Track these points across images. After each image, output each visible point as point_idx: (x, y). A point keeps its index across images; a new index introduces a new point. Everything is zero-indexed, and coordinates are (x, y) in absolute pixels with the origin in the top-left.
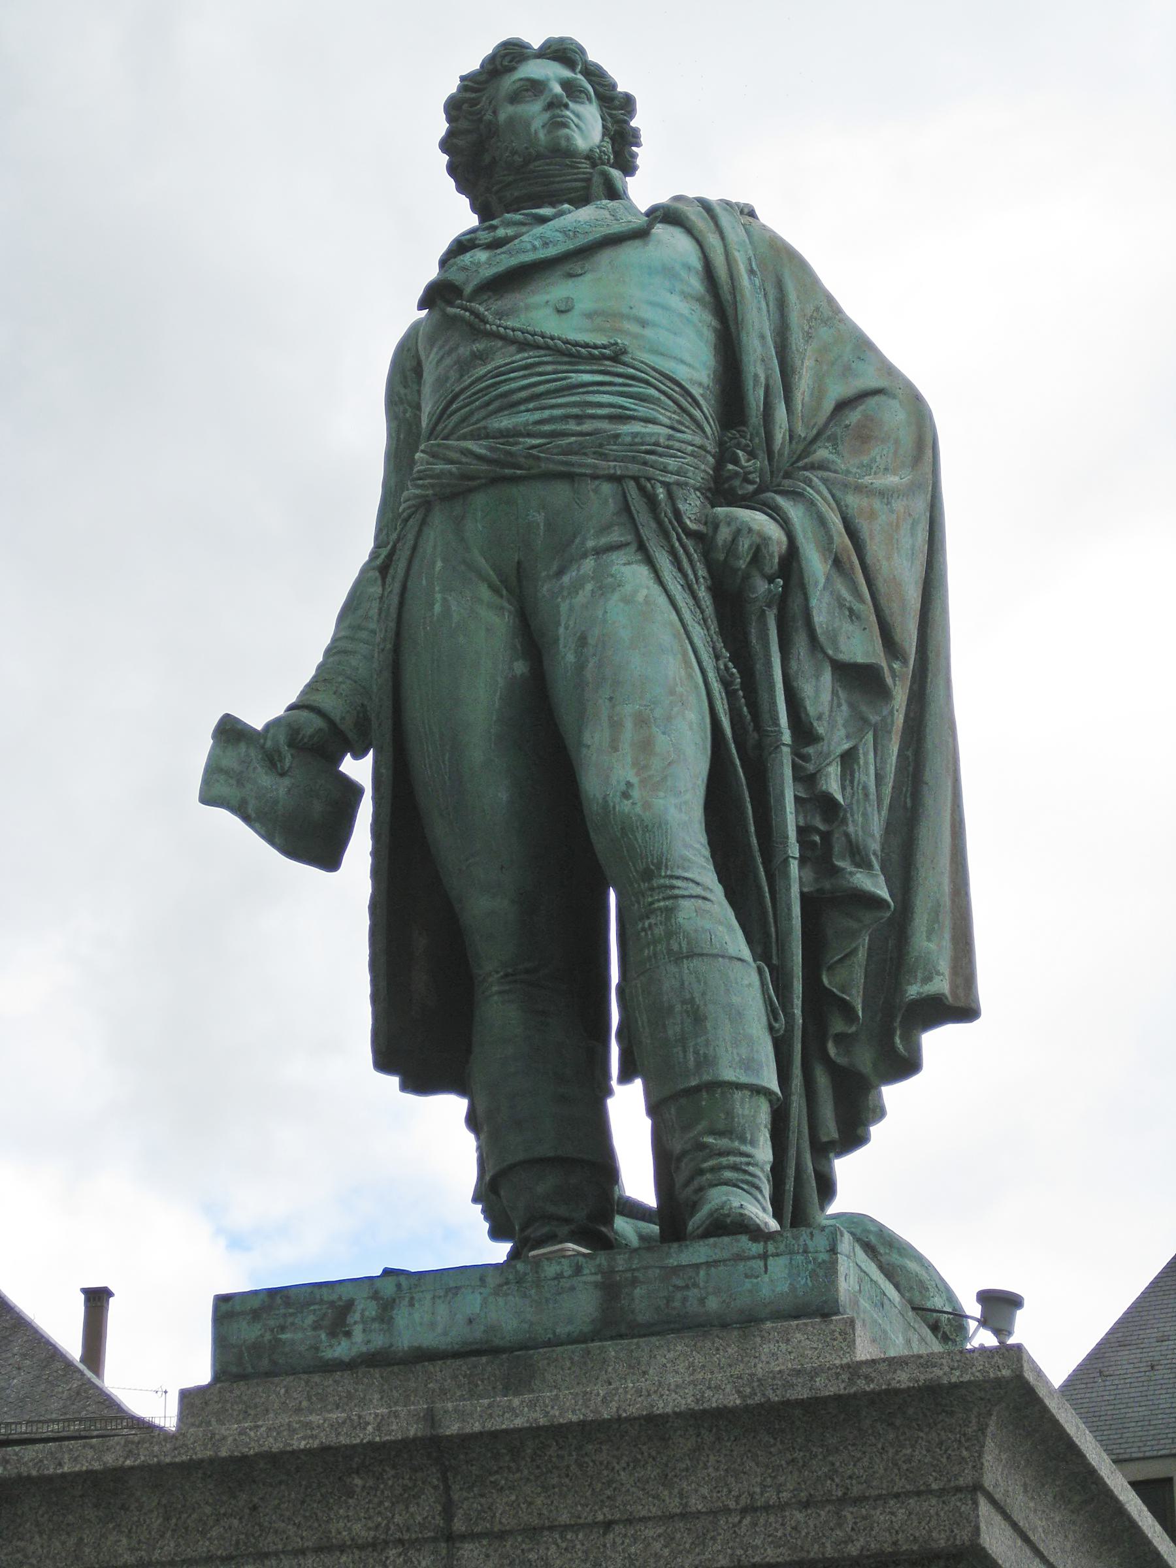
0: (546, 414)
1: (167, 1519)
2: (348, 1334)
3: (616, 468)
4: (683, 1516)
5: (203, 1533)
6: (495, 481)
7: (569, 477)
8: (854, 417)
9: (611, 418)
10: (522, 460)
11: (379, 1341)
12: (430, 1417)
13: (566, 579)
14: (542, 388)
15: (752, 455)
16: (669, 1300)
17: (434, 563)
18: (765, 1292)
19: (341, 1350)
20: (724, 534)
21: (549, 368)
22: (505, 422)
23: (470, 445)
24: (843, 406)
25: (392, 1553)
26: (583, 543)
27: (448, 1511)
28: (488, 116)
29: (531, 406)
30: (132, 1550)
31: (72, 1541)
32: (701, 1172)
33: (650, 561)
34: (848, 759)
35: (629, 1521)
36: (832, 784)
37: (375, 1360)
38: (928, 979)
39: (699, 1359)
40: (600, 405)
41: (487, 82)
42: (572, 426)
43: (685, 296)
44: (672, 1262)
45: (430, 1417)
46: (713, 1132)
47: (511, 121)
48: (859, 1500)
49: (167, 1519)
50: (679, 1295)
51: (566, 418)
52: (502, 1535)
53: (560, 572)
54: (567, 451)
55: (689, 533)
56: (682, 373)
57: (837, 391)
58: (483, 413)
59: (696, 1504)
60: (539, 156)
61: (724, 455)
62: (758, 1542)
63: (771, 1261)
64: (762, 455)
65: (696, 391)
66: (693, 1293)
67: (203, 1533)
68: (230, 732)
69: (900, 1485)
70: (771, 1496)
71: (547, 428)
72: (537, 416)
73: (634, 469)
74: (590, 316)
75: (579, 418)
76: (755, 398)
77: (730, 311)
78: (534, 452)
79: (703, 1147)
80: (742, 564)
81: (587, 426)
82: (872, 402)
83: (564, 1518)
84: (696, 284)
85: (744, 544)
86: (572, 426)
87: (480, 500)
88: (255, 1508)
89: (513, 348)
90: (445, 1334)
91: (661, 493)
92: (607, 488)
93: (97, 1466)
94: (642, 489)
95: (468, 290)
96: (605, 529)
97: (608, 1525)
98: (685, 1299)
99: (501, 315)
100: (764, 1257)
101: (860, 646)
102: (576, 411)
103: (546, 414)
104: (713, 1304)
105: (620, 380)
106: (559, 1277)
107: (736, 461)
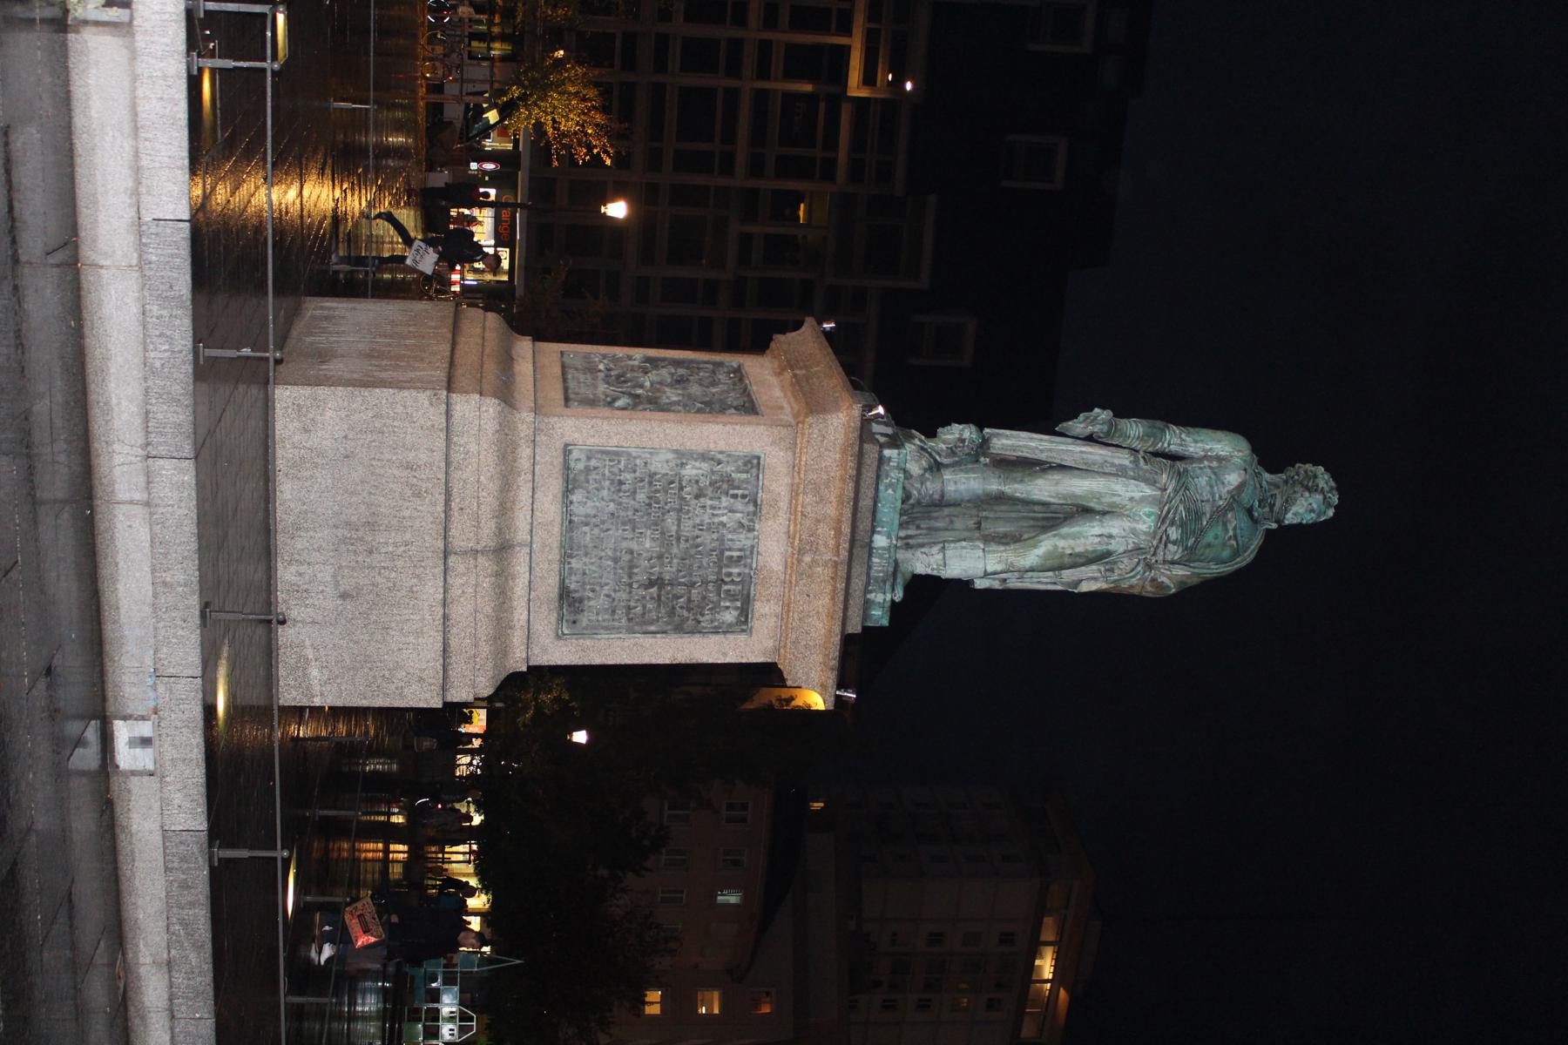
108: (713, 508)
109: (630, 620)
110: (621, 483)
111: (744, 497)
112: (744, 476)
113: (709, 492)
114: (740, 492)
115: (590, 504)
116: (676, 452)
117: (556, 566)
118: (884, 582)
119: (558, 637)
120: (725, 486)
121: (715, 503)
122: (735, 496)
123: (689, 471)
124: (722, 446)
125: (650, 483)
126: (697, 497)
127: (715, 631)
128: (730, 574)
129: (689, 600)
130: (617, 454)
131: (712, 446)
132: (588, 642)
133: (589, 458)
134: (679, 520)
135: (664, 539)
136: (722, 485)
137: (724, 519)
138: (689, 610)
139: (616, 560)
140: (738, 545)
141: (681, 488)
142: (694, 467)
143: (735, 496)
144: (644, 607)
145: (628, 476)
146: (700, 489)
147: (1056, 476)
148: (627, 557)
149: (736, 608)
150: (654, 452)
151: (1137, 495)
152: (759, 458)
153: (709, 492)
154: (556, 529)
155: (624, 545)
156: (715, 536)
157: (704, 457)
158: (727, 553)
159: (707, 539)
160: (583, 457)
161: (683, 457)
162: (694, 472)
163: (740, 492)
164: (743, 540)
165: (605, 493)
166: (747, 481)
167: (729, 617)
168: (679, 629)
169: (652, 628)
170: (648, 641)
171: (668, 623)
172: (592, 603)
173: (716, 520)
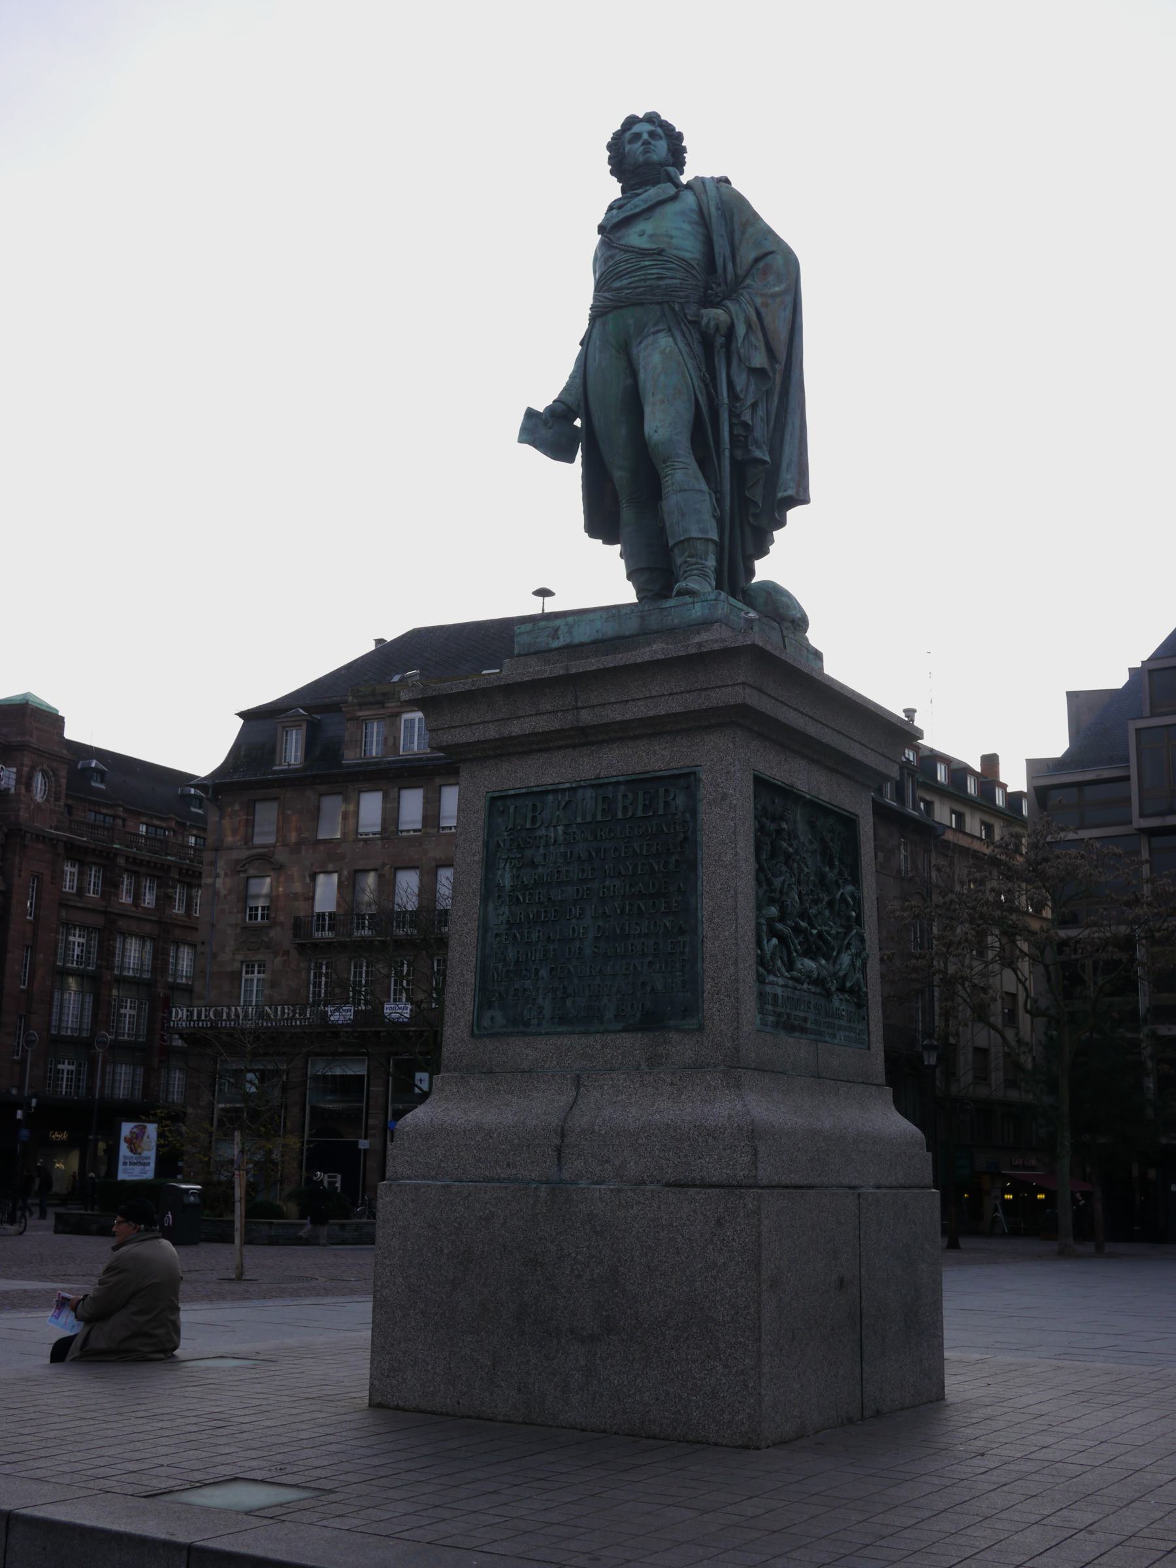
4: (650, 697)
7: (641, 304)
8: (761, 265)
9: (658, 279)
11: (568, 640)
12: (567, 668)
13: (642, 345)
15: (719, 285)
19: (555, 644)
20: (705, 321)
22: (617, 284)
24: (757, 260)
33: (673, 336)
34: (754, 406)
35: (633, 700)
36: (747, 417)
38: (785, 490)
42: (642, 284)
43: (690, 223)
45: (567, 668)
46: (690, 556)
48: (706, 689)
51: (640, 280)
52: (593, 707)
54: (641, 294)
55: (690, 322)
56: (687, 255)
57: (753, 255)
59: (654, 693)
61: (707, 287)
65: (693, 263)
66: (670, 618)
68: (530, 414)
70: (678, 689)
74: (651, 236)
75: (645, 280)
76: (719, 262)
79: (686, 562)
80: (712, 332)
81: (648, 283)
82: (770, 257)
83: (613, 700)
84: (695, 217)
85: (712, 323)
86: (642, 284)
87: (610, 316)
91: (677, 307)
96: (656, 324)
97: (627, 701)
99: (619, 238)
101: (759, 360)
104: (676, 621)
107: (712, 289)
108: (547, 845)
109: (682, 932)
110: (517, 962)
113: (528, 853)
115: (540, 1001)
116: (485, 899)
117: (610, 1037)
119: (701, 1028)
122: (534, 818)
126: (534, 865)
127: (694, 812)
131: (477, 858)
133: (490, 1006)
137: (560, 829)
142: (502, 877)
145: (511, 954)
149: (667, 791)
150: (484, 927)
152: (493, 799)
154: (567, 1041)
157: (489, 865)
162: (508, 875)
173: (561, 838)
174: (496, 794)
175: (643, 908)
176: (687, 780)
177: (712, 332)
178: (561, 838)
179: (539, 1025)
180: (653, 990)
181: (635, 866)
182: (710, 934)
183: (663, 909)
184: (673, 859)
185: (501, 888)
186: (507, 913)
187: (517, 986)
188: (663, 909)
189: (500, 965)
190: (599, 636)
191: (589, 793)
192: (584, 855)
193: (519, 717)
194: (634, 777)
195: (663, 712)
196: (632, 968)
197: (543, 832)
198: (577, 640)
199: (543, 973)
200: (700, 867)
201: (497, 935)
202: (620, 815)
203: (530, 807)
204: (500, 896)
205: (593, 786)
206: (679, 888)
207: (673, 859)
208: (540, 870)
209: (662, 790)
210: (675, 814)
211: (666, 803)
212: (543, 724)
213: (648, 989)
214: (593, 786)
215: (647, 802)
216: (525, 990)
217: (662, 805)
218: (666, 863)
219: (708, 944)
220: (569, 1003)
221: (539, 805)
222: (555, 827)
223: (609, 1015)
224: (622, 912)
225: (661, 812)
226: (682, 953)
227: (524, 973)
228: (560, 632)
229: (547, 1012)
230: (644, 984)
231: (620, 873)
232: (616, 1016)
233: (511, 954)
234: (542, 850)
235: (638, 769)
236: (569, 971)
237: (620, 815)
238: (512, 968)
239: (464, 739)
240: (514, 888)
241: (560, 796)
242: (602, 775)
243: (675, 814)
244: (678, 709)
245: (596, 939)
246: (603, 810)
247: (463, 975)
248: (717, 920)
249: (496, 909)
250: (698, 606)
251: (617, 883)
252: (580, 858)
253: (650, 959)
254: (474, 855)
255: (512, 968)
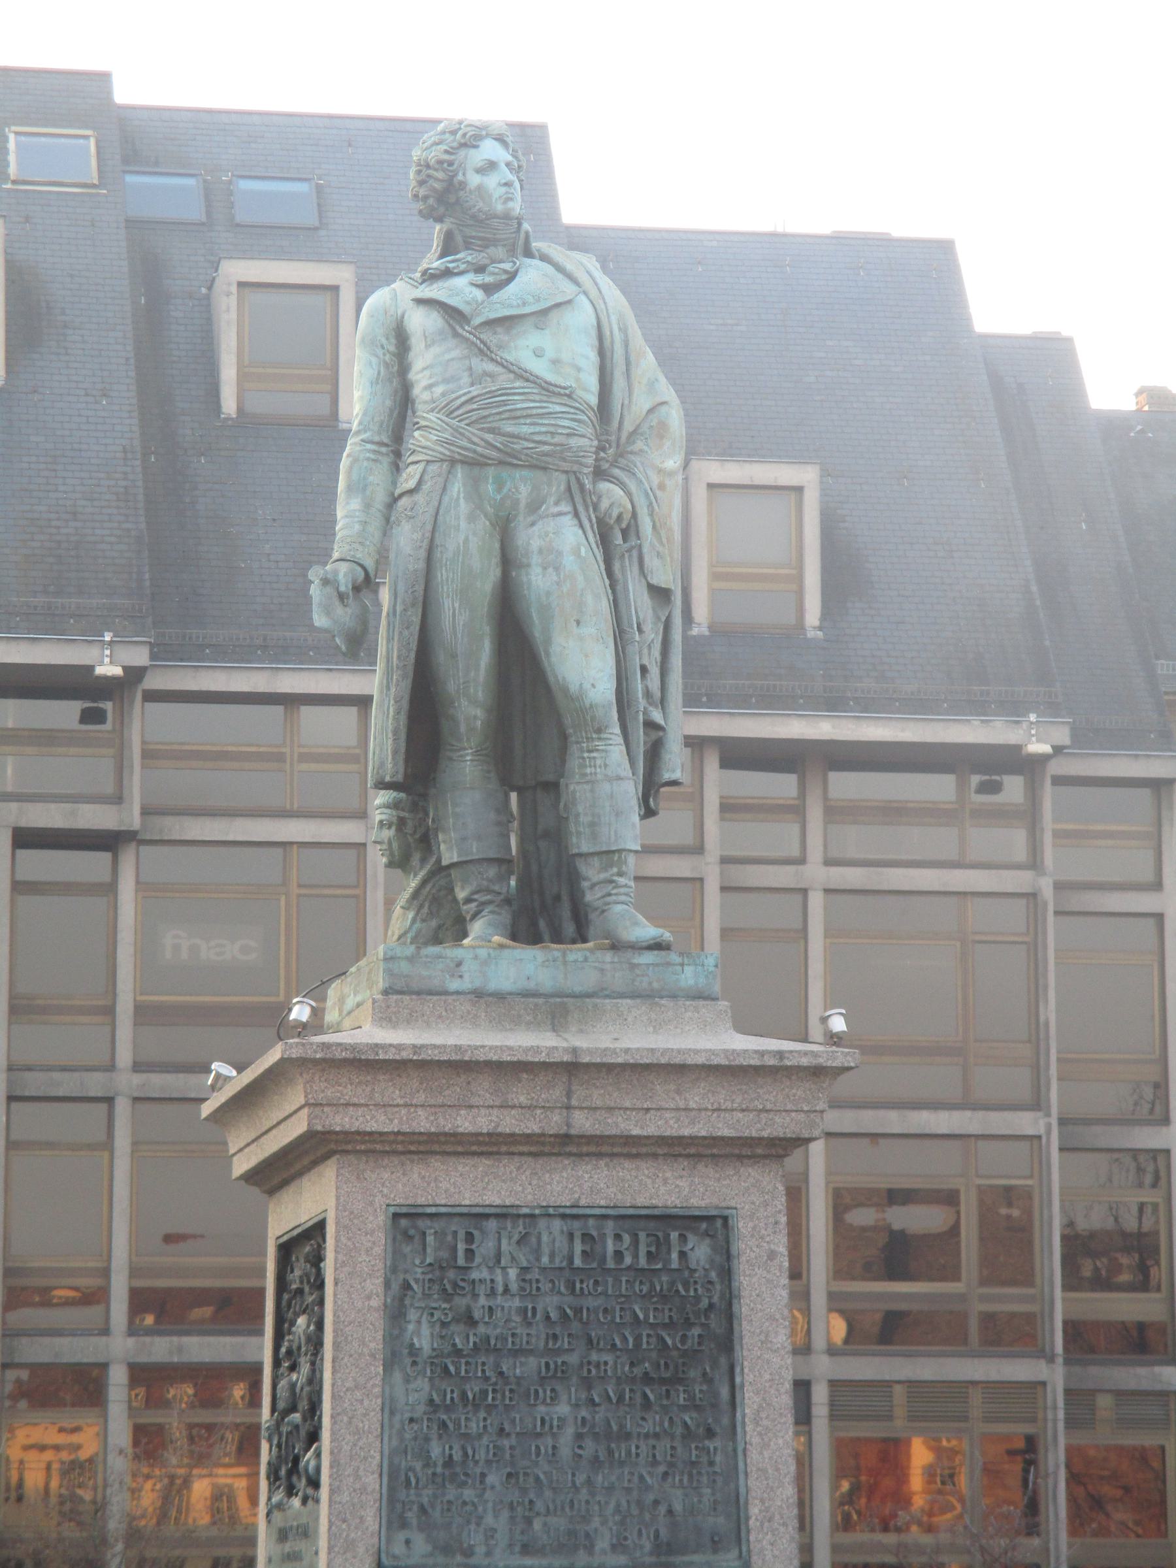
0: (537, 429)
1: (421, 1083)
2: (461, 977)
3: (566, 466)
5: (440, 1093)
6: (501, 463)
7: (545, 469)
8: (654, 420)
10: (523, 457)
14: (534, 411)
16: (634, 980)
17: (457, 505)
18: (683, 984)
19: (454, 985)
20: (604, 505)
21: (537, 398)
22: (509, 428)
23: (489, 437)
24: (651, 411)
25: (538, 1112)
26: (547, 509)
27: (569, 1095)
28: (460, 177)
29: (528, 421)
30: (402, 1097)
31: (369, 1089)
32: (610, 895)
33: (581, 526)
37: (478, 994)
39: (653, 1016)
40: (564, 427)
41: (457, 148)
44: (635, 961)
47: (480, 188)
48: (767, 1111)
49: (421, 1083)
50: (638, 979)
52: (596, 1109)
53: (533, 524)
58: (498, 417)
59: (692, 1105)
60: (496, 216)
62: (720, 1125)
63: (686, 968)
64: (614, 445)
67: (440, 1093)
69: (789, 1107)
70: (729, 1105)
71: (537, 438)
72: (532, 429)
73: (575, 468)
74: (555, 362)
77: (608, 354)
78: (528, 451)
79: (611, 882)
80: (612, 522)
81: (557, 439)
82: (664, 409)
83: (628, 1104)
86: (548, 438)
88: (469, 1083)
89: (512, 376)
90: (515, 983)
92: (563, 477)
93: (398, 1057)
94: (578, 479)
95: (477, 321)
96: (557, 503)
97: (648, 1110)
98: (641, 982)
99: (500, 347)
100: (682, 965)
102: (552, 429)
103: (537, 429)
105: (572, 410)
106: (576, 961)
108: (492, 1293)
109: (710, 1433)
110: (449, 1462)
111: (470, 1237)
112: (430, 1239)
113: (461, 1302)
114: (461, 1247)
115: (489, 1520)
116: (388, 1366)
118: (633, 967)
120: (451, 1274)
121: (482, 1290)
122: (470, 1254)
123: (424, 1337)
124: (375, 1285)
125: (448, 1409)
126: (470, 1321)
127: (727, 1273)
128: (619, 1255)
129: (670, 1325)
130: (393, 1476)
131: (375, 1302)
132: (754, 1511)
133: (404, 1525)
134: (516, 1353)
135: (555, 1375)
136: (449, 1280)
137: (513, 1273)
138: (688, 1323)
139: (596, 1462)
140: (561, 1243)
141: (458, 1352)
142: (417, 1332)
143: (470, 1254)
144: (685, 1408)
145: (436, 1450)
146: (456, 1320)
147: (440, 657)
148: (590, 1446)
149: (683, 1238)
150: (390, 1408)
151: (464, 507)
152: (396, 1216)
153: (461, 1302)
155: (565, 1452)
156: (546, 1286)
157: (396, 1314)
158: (578, 1262)
159: (550, 1303)
160: (401, 1536)
161: (397, 1354)
162: (425, 1330)
163: (461, 1247)
164: (552, 1234)
165: (468, 1494)
166: (440, 1235)
167: (700, 1252)
168: (727, 1343)
169: (724, 1392)
170: (750, 1401)
171: (715, 1364)
172: (678, 1507)
173: (514, 1287)
174: (404, 1210)
175: (651, 1397)
176: (715, 1225)
177: (612, 522)
178: (514, 1287)
179: (488, 1554)
180: (670, 1512)
181: (638, 1339)
182: (755, 1440)
183: (682, 1402)
184: (696, 1331)
185: (413, 1351)
186: (427, 1387)
187: (450, 1497)
188: (682, 1402)
189: (418, 1466)
190: (532, 985)
191: (557, 1224)
192: (554, 1315)
193: (471, 1107)
194: (631, 1212)
195: (703, 1133)
196: (636, 1479)
197: (485, 1274)
198: (493, 986)
199: (492, 1479)
200: (737, 1347)
201: (411, 1420)
202: (611, 1264)
203: (461, 1235)
204: (414, 1363)
205: (564, 1216)
206: (704, 1374)
207: (696, 1331)
208: (482, 1329)
209: (674, 1235)
210: (695, 1270)
211: (683, 1255)
212: (510, 1123)
213: (662, 1509)
214: (564, 1216)
215: (653, 1249)
216: (465, 1503)
217: (674, 1256)
218: (684, 1338)
219: (754, 1455)
220: (537, 1525)
221: (476, 1233)
222: (504, 1269)
223: (602, 1544)
224: (621, 1399)
225: (675, 1265)
226: (711, 1463)
227: (463, 1477)
228: (464, 968)
229: (502, 1538)
230: (656, 1502)
231: (614, 1345)
232: (614, 1547)
233: (436, 1450)
234: (482, 1301)
235: (641, 1201)
236: (537, 1479)
237: (611, 1264)
238: (439, 1470)
239: (372, 1126)
240: (438, 1354)
241: (509, 1224)
242: (583, 1202)
243: (695, 1270)
244: (727, 1132)
245: (579, 1436)
246: (584, 1252)
247: (357, 1477)
248: (765, 1422)
249: (407, 1380)
250: (689, 970)
251: (609, 1358)
252: (548, 1318)
253: (662, 1469)
254: (369, 1298)
255: (439, 1470)
